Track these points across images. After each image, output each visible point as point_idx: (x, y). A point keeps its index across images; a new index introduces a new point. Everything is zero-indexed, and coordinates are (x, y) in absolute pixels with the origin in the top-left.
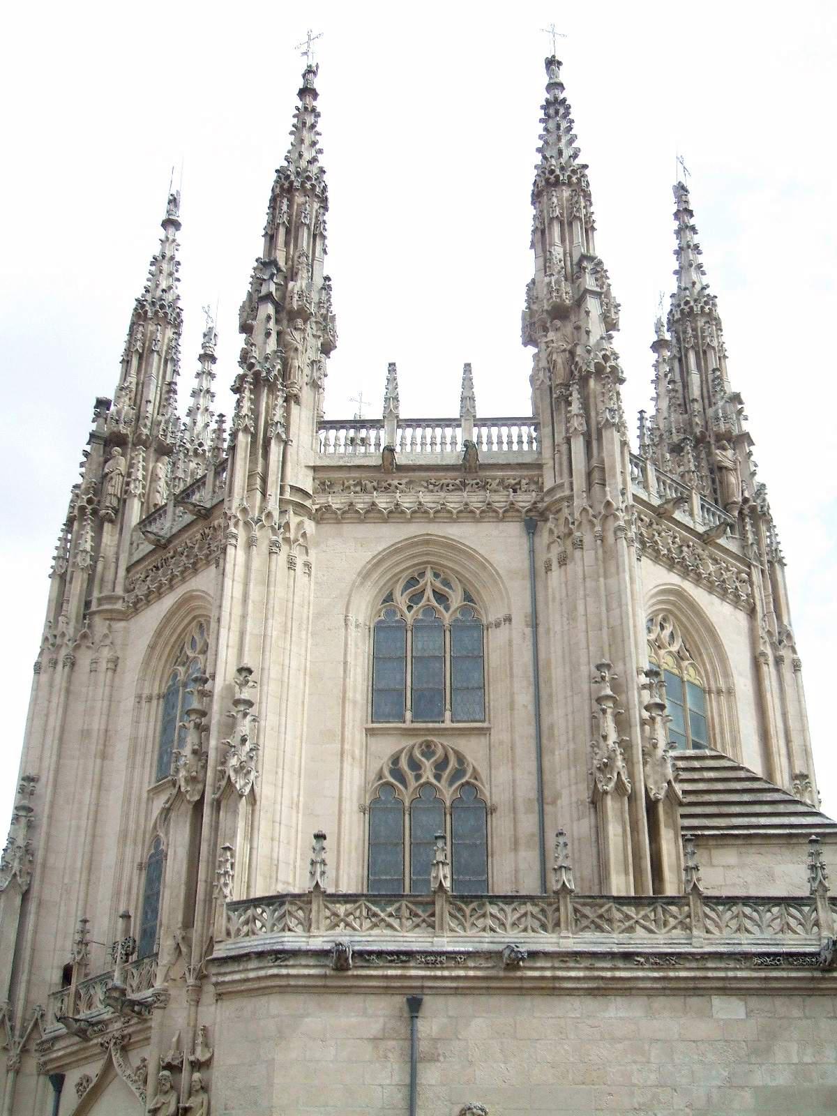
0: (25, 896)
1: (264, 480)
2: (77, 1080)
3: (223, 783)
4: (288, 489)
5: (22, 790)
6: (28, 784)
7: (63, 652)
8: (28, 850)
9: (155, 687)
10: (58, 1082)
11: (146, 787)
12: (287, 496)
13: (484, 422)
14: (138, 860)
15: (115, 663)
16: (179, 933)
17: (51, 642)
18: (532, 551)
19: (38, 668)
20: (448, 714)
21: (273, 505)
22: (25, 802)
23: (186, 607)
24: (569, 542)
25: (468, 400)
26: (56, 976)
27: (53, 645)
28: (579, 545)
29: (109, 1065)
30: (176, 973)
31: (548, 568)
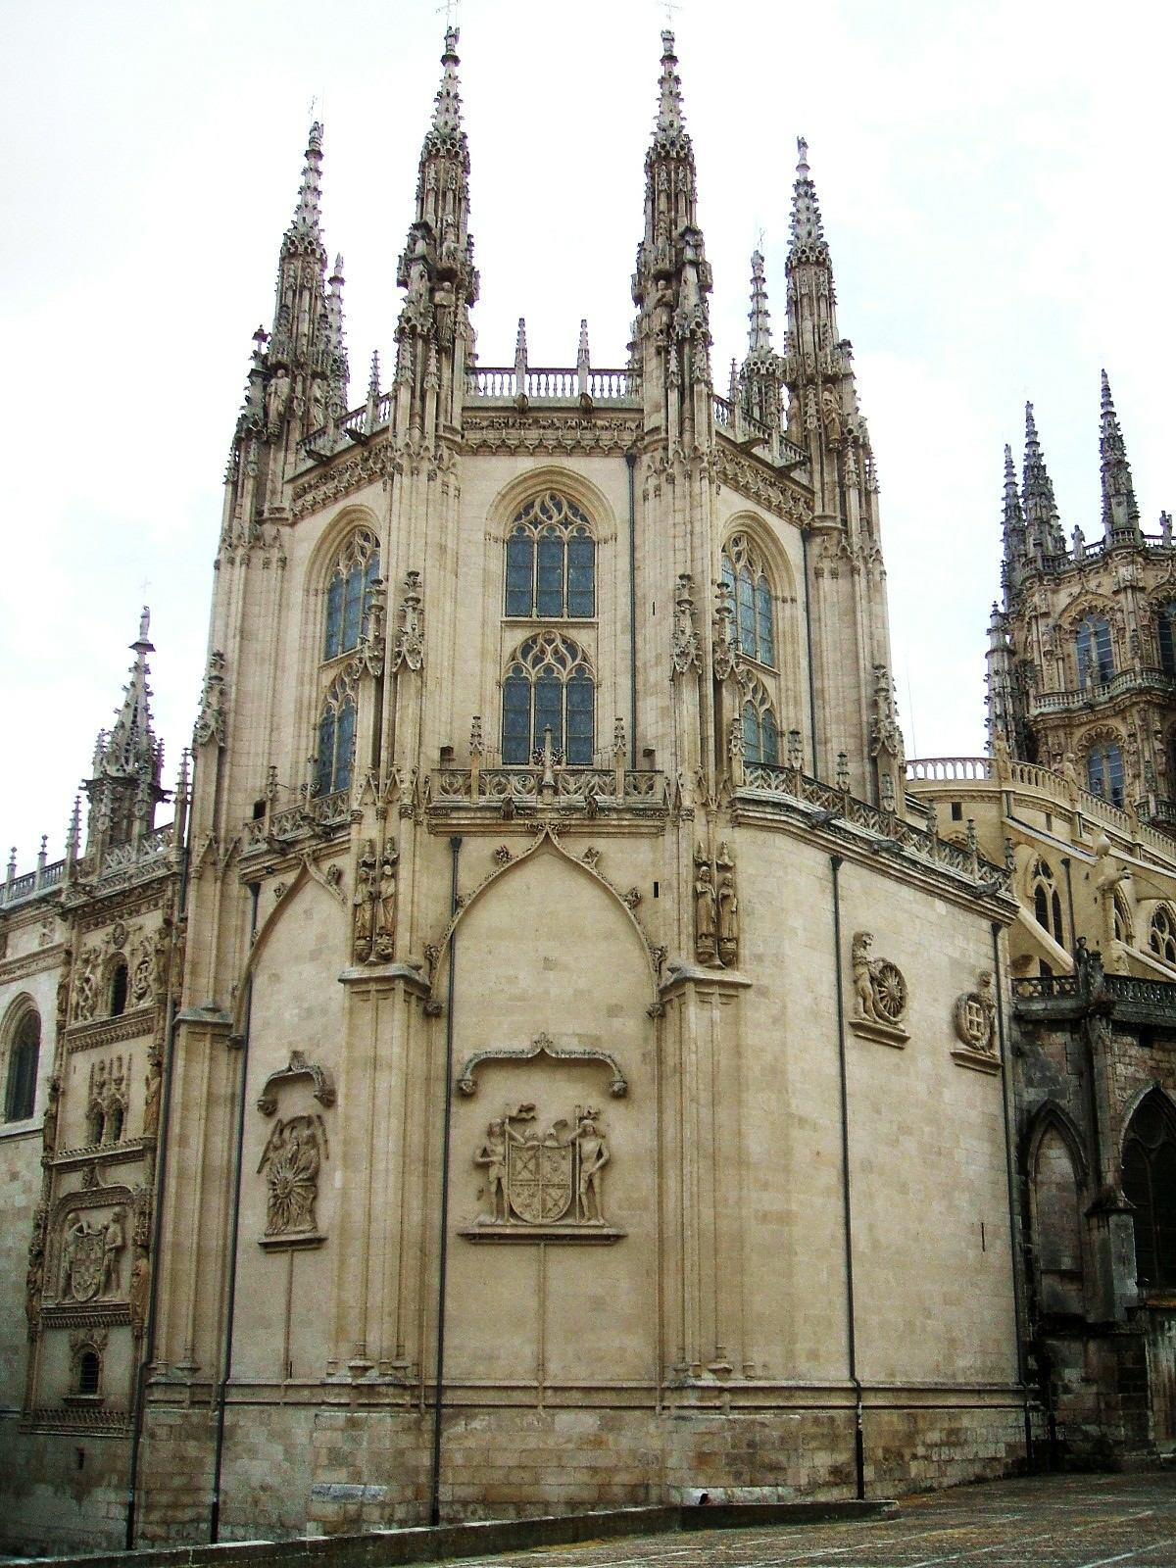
0: (222, 751)
1: (423, 419)
3: (399, 661)
4: (441, 428)
5: (213, 665)
6: (218, 659)
7: (241, 551)
8: (221, 713)
9: (322, 584)
10: (256, 889)
11: (316, 665)
12: (441, 433)
13: (594, 372)
14: (312, 721)
15: (283, 561)
16: (370, 772)
17: (228, 542)
18: (632, 483)
19: (217, 566)
21: (430, 442)
22: (215, 673)
23: (345, 521)
24: (663, 477)
26: (250, 812)
27: (230, 546)
28: (671, 480)
29: (305, 871)
30: (369, 799)
31: (645, 498)
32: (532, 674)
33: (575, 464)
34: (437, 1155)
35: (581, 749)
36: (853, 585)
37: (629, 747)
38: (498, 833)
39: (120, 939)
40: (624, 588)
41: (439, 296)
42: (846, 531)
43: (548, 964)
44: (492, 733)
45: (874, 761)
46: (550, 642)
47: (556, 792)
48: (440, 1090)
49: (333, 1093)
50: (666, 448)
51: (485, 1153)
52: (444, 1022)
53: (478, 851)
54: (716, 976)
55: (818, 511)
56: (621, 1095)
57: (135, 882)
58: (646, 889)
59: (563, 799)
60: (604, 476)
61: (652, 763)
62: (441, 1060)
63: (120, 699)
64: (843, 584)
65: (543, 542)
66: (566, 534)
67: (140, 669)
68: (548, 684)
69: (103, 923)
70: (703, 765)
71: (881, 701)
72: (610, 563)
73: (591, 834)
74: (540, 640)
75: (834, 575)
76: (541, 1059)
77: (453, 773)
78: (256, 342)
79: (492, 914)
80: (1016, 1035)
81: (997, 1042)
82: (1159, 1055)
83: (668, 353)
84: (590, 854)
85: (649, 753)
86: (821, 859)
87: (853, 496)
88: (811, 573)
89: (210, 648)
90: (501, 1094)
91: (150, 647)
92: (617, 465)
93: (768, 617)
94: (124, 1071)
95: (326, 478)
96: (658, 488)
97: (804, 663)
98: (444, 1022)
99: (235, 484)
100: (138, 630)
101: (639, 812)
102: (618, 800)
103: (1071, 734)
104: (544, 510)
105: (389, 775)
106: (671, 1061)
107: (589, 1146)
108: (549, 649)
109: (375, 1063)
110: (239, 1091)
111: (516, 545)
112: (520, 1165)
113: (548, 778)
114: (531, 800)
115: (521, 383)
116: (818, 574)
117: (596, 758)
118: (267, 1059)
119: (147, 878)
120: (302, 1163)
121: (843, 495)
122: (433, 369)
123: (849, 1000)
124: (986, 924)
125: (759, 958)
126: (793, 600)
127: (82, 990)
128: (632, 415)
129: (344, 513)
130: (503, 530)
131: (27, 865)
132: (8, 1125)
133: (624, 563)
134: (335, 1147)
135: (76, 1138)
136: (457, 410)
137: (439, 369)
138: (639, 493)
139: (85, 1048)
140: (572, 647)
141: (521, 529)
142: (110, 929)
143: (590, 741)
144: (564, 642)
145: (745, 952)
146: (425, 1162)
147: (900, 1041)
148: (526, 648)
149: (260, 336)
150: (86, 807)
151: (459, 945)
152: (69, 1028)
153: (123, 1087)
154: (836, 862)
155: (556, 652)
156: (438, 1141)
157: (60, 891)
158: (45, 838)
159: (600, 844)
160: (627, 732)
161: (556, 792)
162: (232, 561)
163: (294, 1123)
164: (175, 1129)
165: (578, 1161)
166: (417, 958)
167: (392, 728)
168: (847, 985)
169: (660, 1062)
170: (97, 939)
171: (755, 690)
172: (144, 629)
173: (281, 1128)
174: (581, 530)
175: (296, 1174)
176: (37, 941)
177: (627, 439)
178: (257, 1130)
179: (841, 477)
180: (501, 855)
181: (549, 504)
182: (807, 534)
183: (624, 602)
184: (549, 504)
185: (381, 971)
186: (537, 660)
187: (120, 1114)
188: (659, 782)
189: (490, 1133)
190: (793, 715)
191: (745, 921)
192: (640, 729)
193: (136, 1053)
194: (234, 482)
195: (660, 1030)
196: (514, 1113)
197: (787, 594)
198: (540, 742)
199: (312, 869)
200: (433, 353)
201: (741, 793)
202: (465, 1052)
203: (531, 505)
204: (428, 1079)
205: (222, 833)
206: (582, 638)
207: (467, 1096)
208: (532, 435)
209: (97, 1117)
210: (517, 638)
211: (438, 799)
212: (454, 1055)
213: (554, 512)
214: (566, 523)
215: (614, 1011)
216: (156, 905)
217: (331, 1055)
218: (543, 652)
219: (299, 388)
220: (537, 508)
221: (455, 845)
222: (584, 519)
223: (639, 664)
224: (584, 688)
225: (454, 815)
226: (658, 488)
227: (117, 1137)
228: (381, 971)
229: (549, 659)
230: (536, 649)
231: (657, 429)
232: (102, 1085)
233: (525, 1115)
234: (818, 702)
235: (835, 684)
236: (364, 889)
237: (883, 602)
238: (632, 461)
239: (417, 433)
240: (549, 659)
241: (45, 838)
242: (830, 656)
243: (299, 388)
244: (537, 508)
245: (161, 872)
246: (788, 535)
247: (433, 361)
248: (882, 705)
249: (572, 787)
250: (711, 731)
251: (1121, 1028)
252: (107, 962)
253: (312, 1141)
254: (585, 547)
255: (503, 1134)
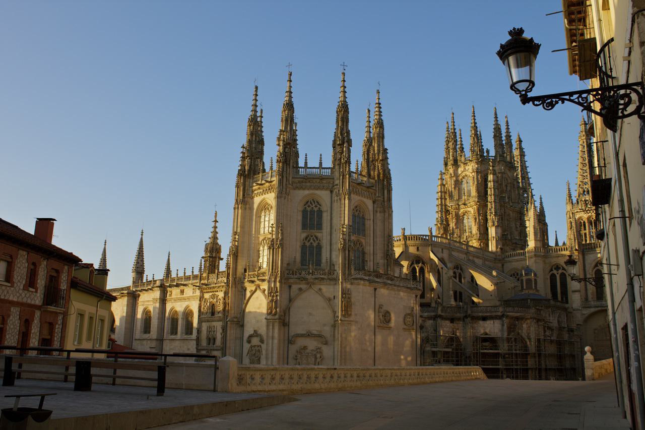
2: (250, 290)
19: (235, 208)
20: (315, 229)
21: (284, 190)
25: (321, 163)
32: (308, 244)
33: (318, 192)
34: (286, 356)
35: (319, 263)
36: (385, 215)
37: (329, 263)
38: (300, 284)
39: (213, 297)
40: (329, 224)
41: (287, 149)
42: (384, 201)
43: (310, 314)
44: (298, 258)
45: (387, 260)
46: (312, 236)
47: (312, 275)
48: (287, 342)
49: (263, 341)
50: (339, 191)
51: (296, 356)
52: (287, 327)
53: (295, 288)
54: (346, 319)
55: (377, 195)
56: (326, 343)
57: (217, 285)
58: (332, 297)
59: (314, 277)
60: (323, 196)
61: (334, 267)
62: (287, 335)
63: (211, 235)
64: (382, 214)
65: (311, 211)
66: (316, 209)
67: (215, 227)
68: (311, 246)
69: (209, 292)
70: (345, 270)
71: (389, 245)
72: (326, 217)
73: (320, 285)
74: (310, 236)
75: (380, 212)
76: (309, 335)
77: (290, 270)
78: (242, 149)
79: (298, 303)
80: (420, 321)
81: (415, 324)
82: (455, 325)
83: (340, 166)
84: (320, 289)
85: (334, 265)
86: (372, 289)
87: (386, 192)
88: (375, 213)
89: (233, 230)
90: (301, 342)
91: (218, 222)
92: (328, 192)
93: (364, 224)
94: (215, 329)
95: (259, 188)
96: (337, 200)
97: (372, 235)
98: (287, 327)
99: (238, 188)
100: (214, 217)
101: (330, 279)
102: (326, 277)
103: (459, 211)
104: (311, 203)
105: (275, 272)
106: (336, 337)
107: (318, 356)
108: (312, 238)
109: (273, 338)
110: (242, 336)
111: (304, 212)
112: (304, 359)
113: (311, 271)
114: (307, 276)
115: (306, 171)
116: (376, 212)
117: (322, 265)
118: (249, 331)
119: (219, 285)
120: (257, 355)
121: (383, 191)
122: (285, 170)
123: (377, 320)
124: (414, 296)
125: (356, 315)
126: (370, 220)
127: (204, 308)
128: (331, 180)
129: (264, 199)
130: (301, 208)
131: (189, 273)
132: (186, 336)
133: (329, 218)
134: (264, 352)
135: (204, 343)
136: (291, 179)
137: (287, 170)
138: (333, 199)
139: (205, 322)
140: (317, 238)
141: (306, 208)
142: (211, 294)
143: (320, 261)
144: (315, 236)
145: (353, 313)
146: (283, 358)
147: (390, 328)
148: (306, 238)
149: (243, 147)
150: (203, 263)
151: (291, 310)
152: (201, 317)
153: (215, 333)
154: (375, 289)
155: (313, 239)
156: (286, 353)
157: (197, 283)
158: (193, 268)
159: (322, 287)
160: (329, 260)
161: (312, 275)
162: (238, 208)
163: (254, 346)
164: (228, 345)
165: (316, 358)
166: (282, 314)
167: (276, 262)
168: (377, 317)
169: (334, 337)
170: (207, 296)
171: (360, 244)
172: (216, 216)
173: (251, 347)
174: (319, 208)
175: (256, 358)
176: (192, 293)
177: (331, 186)
178: (246, 346)
179: (383, 186)
180: (300, 289)
181: (312, 201)
182: (374, 202)
183: (329, 227)
184: (312, 201)
185: (273, 317)
186: (309, 241)
187: (214, 339)
188: (336, 273)
189: (297, 352)
190: (369, 249)
191: (353, 307)
192: (332, 258)
193: (218, 325)
194: (237, 186)
195: (334, 330)
196: (302, 348)
197: (369, 218)
198: (309, 261)
199: (258, 288)
200: (285, 166)
201: (353, 277)
202: (292, 333)
203: (308, 201)
204: (284, 341)
205: (237, 276)
206: (319, 235)
207: (291, 343)
208: (308, 184)
209: (209, 340)
210: (304, 235)
211: (286, 275)
212: (290, 334)
213: (313, 203)
214: (316, 206)
215: (324, 325)
216: (222, 291)
217: (263, 331)
218: (310, 239)
219: (253, 162)
220: (309, 203)
221: (290, 287)
222: (320, 205)
223: (332, 243)
224: (319, 247)
225: (290, 280)
226: (337, 200)
227: (214, 344)
228: (273, 317)
229: (312, 241)
230: (309, 238)
231: (337, 185)
232: (210, 332)
233: (305, 348)
234: (375, 244)
235: (379, 240)
236: (270, 298)
237: (392, 219)
238: (331, 192)
239: (281, 187)
240: (312, 241)
241: (193, 268)
242: (379, 233)
243: (253, 162)
244: (309, 203)
245: (223, 284)
246: (369, 203)
247: (285, 168)
248: (390, 246)
249: (316, 274)
250: (347, 262)
251: (446, 319)
252: (210, 303)
253: (259, 351)
254: (320, 213)
255: (300, 352)
